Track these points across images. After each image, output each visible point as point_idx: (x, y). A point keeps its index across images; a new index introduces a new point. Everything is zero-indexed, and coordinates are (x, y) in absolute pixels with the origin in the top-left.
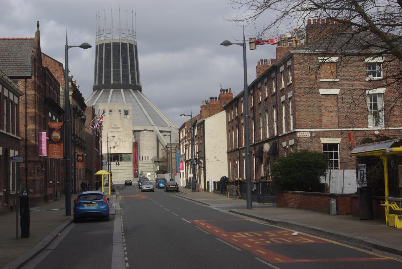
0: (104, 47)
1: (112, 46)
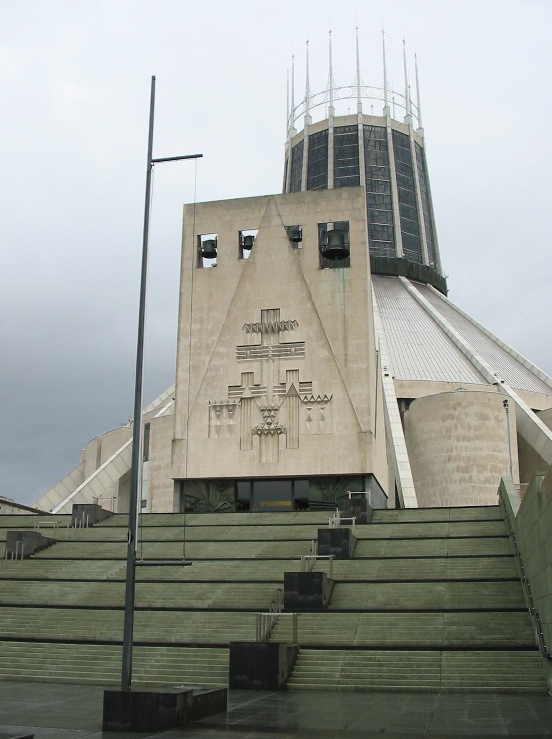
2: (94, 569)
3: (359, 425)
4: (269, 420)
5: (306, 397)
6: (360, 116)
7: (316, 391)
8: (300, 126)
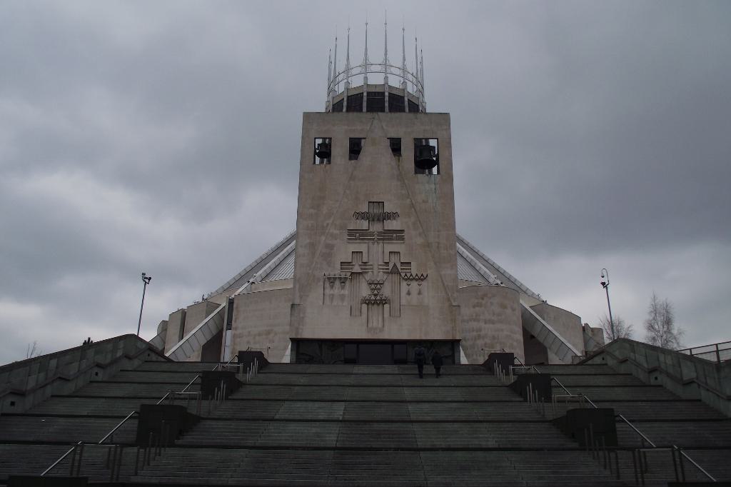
0: (345, 104)
1: (365, 99)
2: (321, 410)
3: (449, 300)
4: (376, 292)
5: (406, 275)
6: (386, 86)
7: (414, 270)
8: (341, 88)
